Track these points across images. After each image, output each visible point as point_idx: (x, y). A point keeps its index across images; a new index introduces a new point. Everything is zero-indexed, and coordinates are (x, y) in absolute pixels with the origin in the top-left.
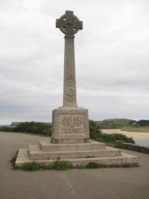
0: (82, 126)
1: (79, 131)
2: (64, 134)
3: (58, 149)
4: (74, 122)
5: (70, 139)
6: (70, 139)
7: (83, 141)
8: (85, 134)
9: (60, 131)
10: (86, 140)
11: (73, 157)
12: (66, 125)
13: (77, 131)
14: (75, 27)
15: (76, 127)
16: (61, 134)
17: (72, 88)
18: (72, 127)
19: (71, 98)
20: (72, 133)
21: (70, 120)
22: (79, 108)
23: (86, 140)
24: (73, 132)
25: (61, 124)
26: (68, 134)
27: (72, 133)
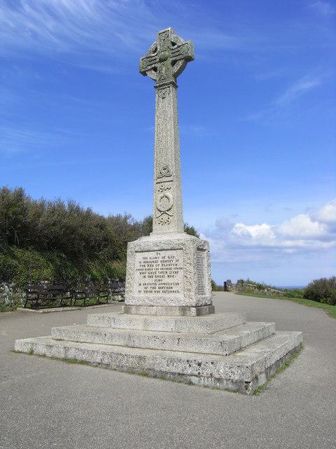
0: (179, 278)
2: (142, 295)
3: (112, 324)
4: (163, 267)
7: (178, 313)
9: (136, 288)
11: (117, 343)
12: (147, 275)
13: (168, 289)
14: (174, 59)
15: (166, 280)
16: (136, 295)
19: (165, 217)
21: (155, 264)
23: (184, 310)
24: (161, 290)
26: (151, 294)
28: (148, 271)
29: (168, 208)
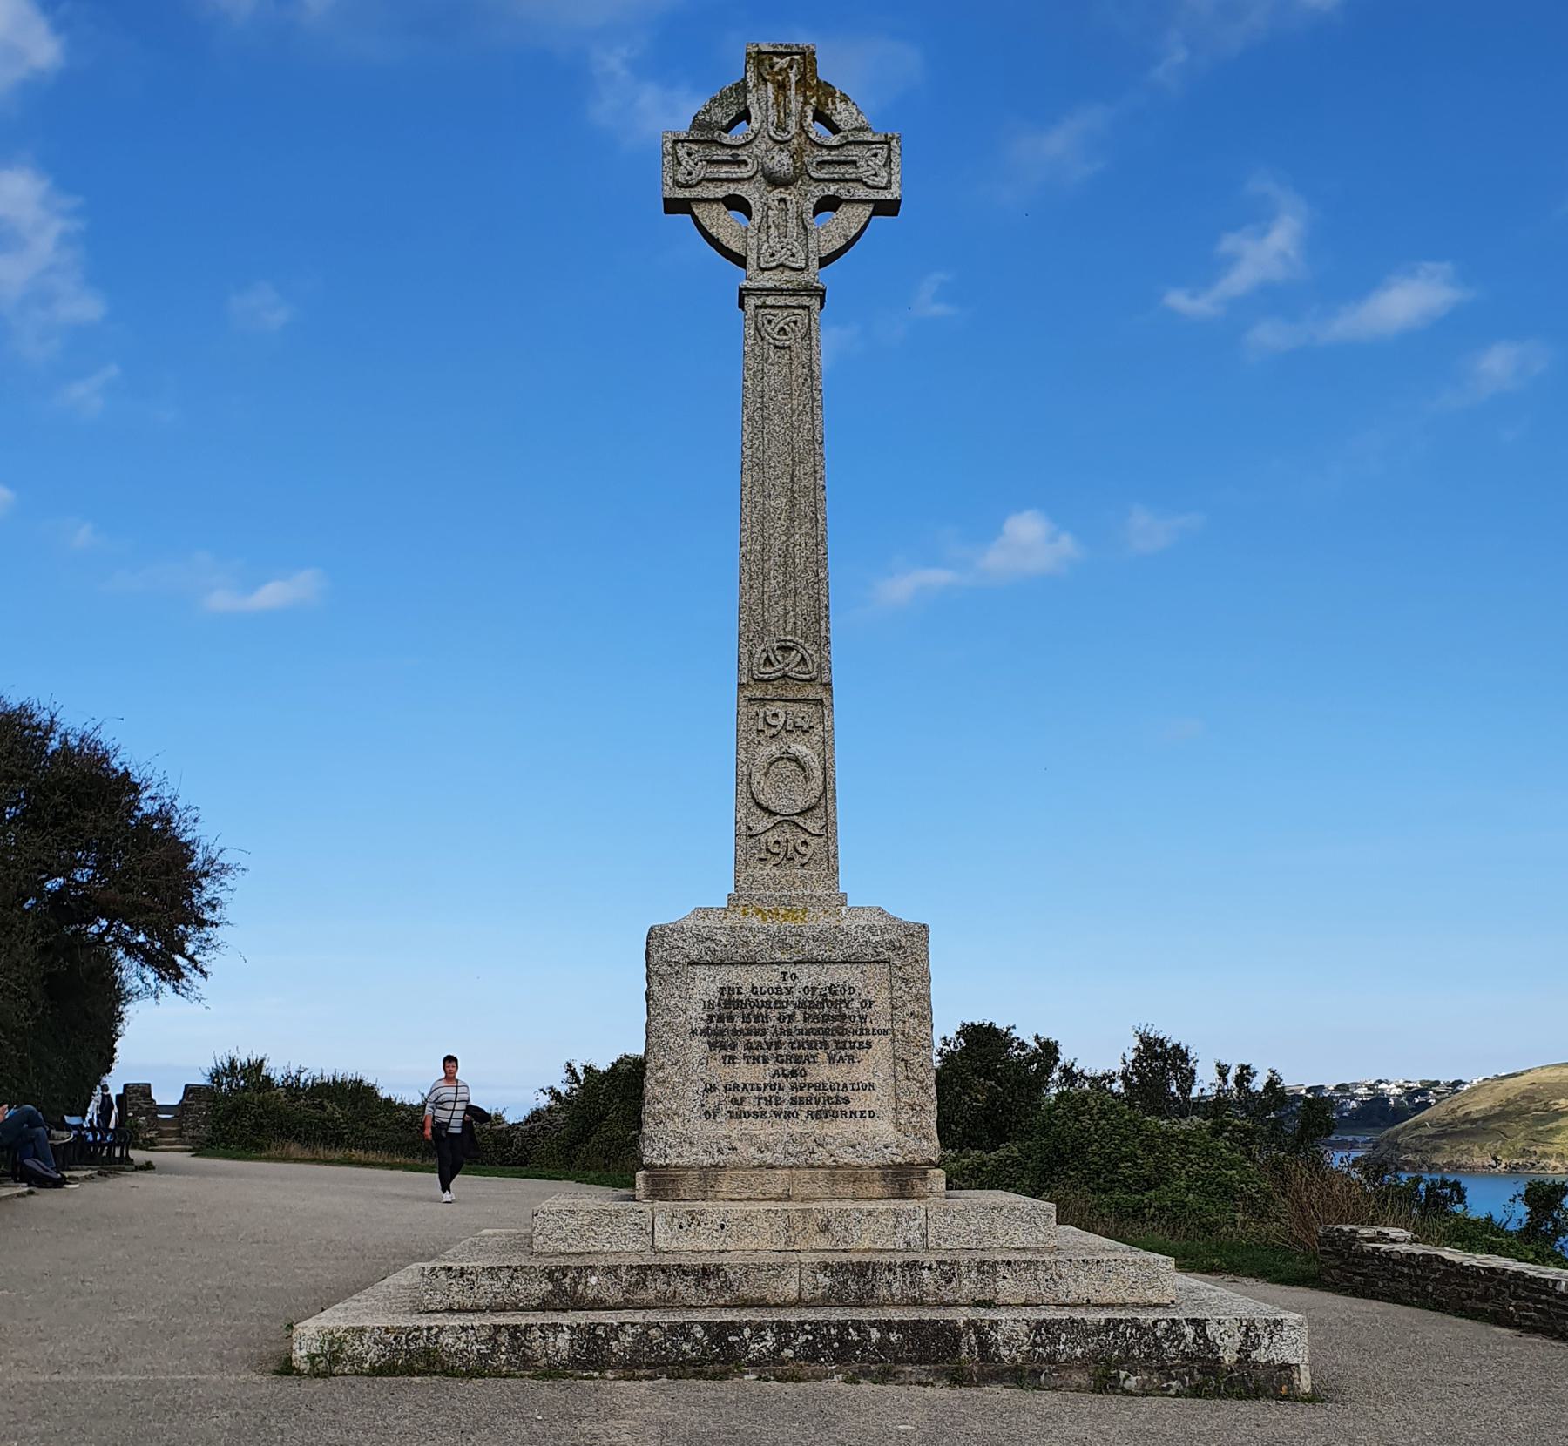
1: (847, 1101)
5: (772, 1167)
6: (772, 1167)
8: (898, 1124)
10: (902, 1178)
13: (829, 1104)
14: (832, 189)
15: (822, 1072)
17: (799, 749)
18: (789, 1067)
20: (788, 1115)
22: (855, 912)
25: (699, 1046)
27: (788, 1115)
28: (741, 1041)
29: (801, 803)
